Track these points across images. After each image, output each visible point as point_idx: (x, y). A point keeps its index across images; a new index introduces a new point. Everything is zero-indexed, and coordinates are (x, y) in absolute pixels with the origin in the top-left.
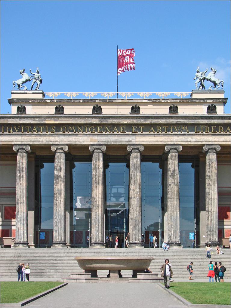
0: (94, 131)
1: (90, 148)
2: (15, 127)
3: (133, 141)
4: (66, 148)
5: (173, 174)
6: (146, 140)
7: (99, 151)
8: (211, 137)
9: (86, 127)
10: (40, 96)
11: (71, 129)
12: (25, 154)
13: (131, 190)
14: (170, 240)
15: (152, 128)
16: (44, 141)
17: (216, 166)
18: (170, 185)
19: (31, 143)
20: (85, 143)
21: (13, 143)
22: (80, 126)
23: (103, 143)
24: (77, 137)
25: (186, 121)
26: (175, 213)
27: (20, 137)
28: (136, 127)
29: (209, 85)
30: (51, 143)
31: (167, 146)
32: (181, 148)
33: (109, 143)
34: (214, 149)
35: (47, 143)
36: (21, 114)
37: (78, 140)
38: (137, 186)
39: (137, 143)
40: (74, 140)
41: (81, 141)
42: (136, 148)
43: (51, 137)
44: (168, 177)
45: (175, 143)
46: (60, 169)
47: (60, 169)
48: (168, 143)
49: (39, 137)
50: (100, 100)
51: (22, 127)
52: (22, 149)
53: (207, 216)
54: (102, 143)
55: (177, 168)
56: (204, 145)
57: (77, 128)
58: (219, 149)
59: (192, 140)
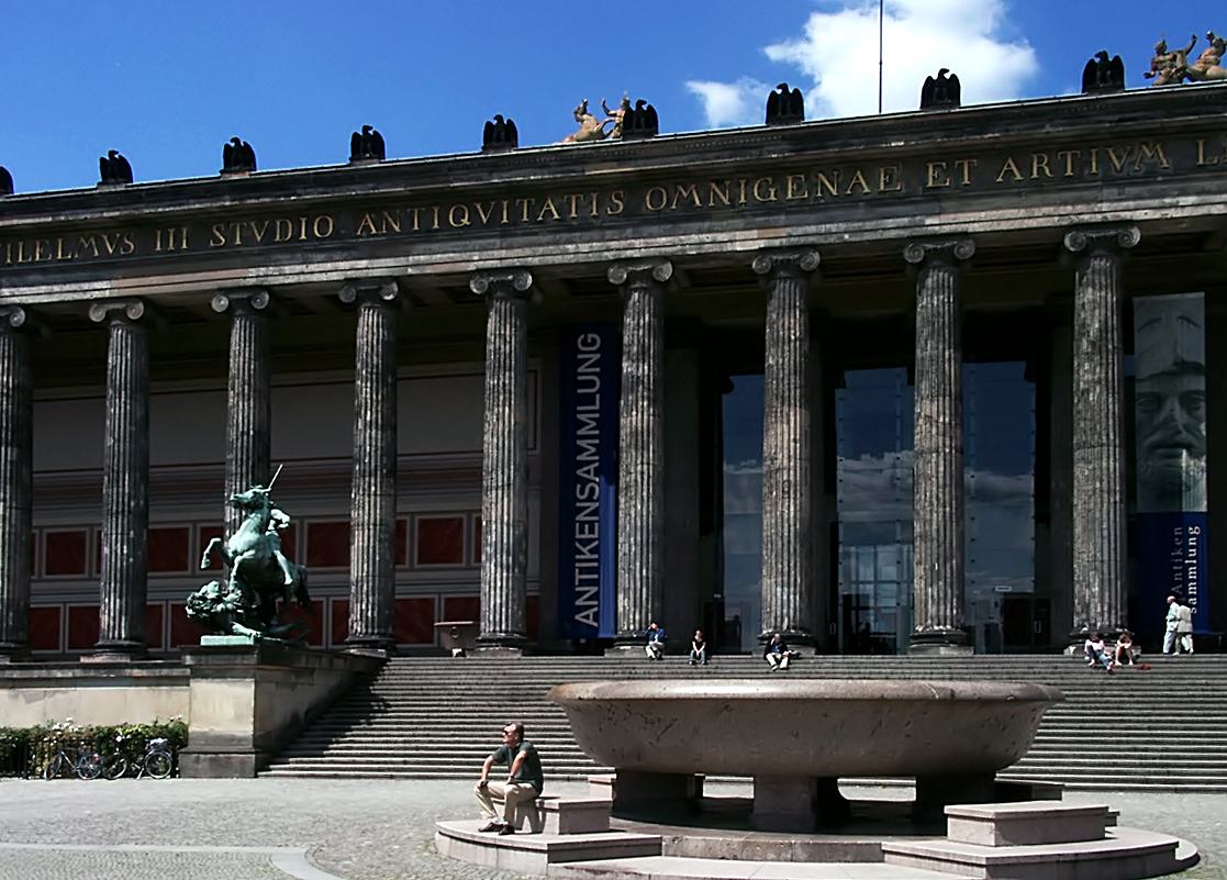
0: (772, 194)
2: (479, 207)
9: (743, 182)
11: (685, 194)
13: (921, 421)
14: (1088, 619)
15: (1010, 161)
18: (1087, 391)
22: (718, 182)
28: (944, 164)
44: (1076, 363)
47: (643, 351)
51: (505, 203)
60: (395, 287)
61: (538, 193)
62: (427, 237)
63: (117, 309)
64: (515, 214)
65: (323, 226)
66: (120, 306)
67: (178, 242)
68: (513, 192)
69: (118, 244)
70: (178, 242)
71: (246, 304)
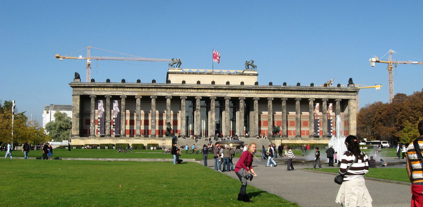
1: (210, 98)
5: (242, 109)
6: (231, 95)
7: (214, 99)
8: (256, 94)
10: (181, 71)
19: (187, 96)
20: (208, 96)
21: (180, 96)
23: (216, 96)
24: (205, 93)
25: (247, 88)
26: (243, 124)
27: (183, 93)
30: (195, 96)
34: (258, 99)
35: (193, 96)
37: (205, 95)
38: (228, 113)
40: (204, 95)
43: (195, 93)
45: (243, 96)
47: (199, 106)
48: (240, 96)
49: (191, 93)
50: (206, 73)
52: (184, 98)
53: (254, 125)
54: (215, 96)
56: (253, 98)
58: (259, 99)
60: (172, 97)
61: (187, 89)
62: (176, 92)
63: (138, 97)
66: (139, 96)
68: (185, 88)
71: (155, 97)
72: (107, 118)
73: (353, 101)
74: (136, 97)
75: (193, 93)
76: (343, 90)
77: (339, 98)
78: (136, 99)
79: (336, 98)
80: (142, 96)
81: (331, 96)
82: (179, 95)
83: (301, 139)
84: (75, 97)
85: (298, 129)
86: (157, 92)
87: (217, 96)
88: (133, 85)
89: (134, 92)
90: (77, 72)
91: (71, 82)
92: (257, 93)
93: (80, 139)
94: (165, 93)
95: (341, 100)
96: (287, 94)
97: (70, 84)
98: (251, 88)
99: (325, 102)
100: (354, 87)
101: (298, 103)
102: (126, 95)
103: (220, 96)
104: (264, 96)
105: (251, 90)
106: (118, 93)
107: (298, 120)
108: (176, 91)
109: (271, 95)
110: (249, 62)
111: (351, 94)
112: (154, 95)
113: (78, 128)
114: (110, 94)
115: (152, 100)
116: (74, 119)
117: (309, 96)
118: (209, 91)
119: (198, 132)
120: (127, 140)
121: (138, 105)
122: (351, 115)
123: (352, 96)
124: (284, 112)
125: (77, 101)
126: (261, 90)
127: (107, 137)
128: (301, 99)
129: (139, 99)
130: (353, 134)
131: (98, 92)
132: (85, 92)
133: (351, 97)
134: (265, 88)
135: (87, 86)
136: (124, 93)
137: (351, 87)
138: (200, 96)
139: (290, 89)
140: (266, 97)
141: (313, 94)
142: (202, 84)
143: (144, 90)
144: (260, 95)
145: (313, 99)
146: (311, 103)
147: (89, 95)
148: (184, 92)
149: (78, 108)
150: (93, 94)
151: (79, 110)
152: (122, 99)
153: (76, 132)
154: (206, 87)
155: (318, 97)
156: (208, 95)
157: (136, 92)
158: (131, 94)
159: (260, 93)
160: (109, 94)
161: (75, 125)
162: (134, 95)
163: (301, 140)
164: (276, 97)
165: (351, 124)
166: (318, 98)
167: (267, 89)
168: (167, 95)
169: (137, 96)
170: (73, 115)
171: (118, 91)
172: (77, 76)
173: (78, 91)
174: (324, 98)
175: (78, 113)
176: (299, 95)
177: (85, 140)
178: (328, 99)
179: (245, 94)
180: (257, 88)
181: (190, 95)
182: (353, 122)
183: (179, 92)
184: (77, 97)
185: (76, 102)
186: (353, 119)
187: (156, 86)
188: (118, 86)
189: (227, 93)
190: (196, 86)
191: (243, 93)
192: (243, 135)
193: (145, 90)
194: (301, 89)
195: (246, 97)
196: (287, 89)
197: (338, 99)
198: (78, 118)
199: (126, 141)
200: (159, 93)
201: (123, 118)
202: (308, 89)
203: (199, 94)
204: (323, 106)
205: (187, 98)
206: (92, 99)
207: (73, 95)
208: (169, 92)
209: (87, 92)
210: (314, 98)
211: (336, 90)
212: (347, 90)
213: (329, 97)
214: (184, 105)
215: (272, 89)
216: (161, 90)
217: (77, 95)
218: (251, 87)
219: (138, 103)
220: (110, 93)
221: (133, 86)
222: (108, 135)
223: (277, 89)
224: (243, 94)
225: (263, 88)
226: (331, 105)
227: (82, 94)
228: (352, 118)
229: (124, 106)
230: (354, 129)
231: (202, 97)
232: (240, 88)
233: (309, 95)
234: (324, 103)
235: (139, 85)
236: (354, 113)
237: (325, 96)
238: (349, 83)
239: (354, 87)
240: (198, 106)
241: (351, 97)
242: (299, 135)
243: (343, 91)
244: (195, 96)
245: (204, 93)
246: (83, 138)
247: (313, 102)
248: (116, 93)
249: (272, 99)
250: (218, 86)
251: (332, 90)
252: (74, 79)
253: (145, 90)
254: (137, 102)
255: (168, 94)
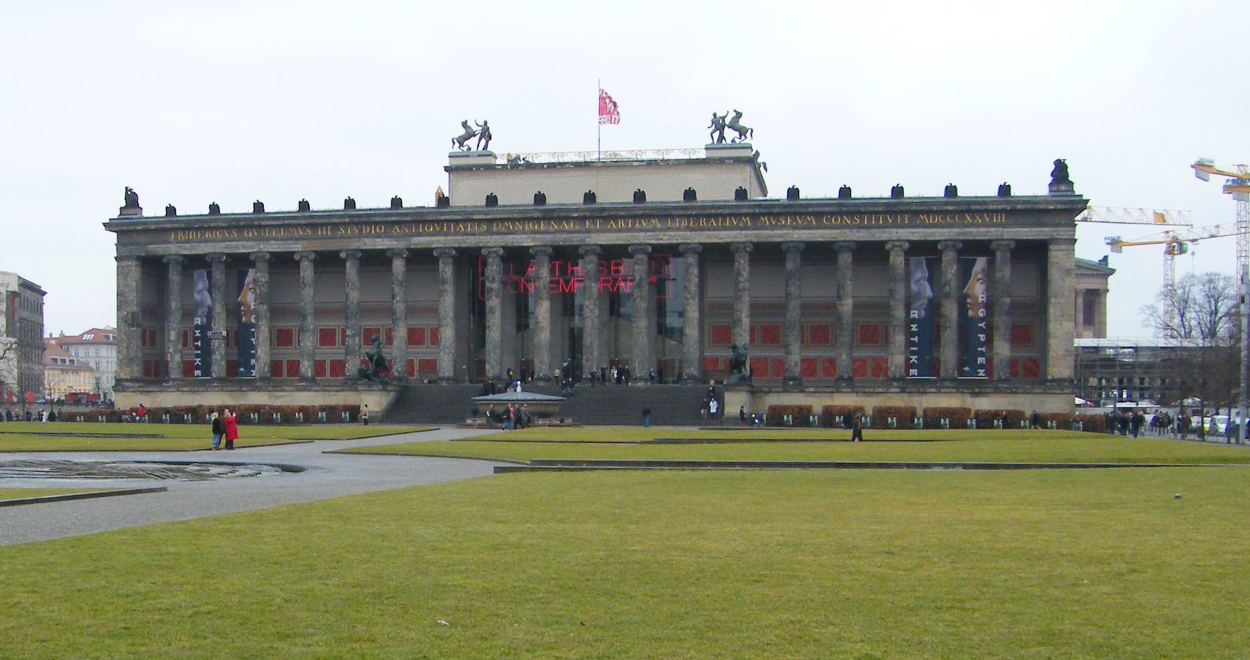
1: (530, 251)
3: (587, 240)
4: (501, 252)
8: (689, 233)
12: (450, 260)
16: (473, 242)
17: (696, 272)
20: (525, 244)
21: (433, 246)
23: (550, 243)
24: (514, 236)
25: (654, 212)
27: (443, 238)
29: (730, 134)
30: (481, 245)
31: (633, 247)
32: (650, 249)
33: (556, 244)
35: (476, 246)
36: (443, 208)
37: (515, 240)
39: (593, 243)
40: (511, 241)
41: (520, 241)
42: (590, 249)
43: (482, 237)
45: (643, 241)
46: (493, 281)
48: (632, 242)
55: (644, 276)
56: (678, 245)
57: (515, 224)
59: (664, 238)
60: (407, 253)
61: (457, 222)
62: (419, 235)
63: (304, 255)
64: (449, 228)
65: (380, 228)
66: (305, 254)
67: (327, 231)
69: (304, 231)
70: (327, 231)
71: (353, 255)
72: (215, 325)
73: (1063, 247)
74: (297, 257)
75: (474, 237)
76: (1019, 207)
77: (1005, 237)
78: (297, 264)
79: (995, 237)
80: (316, 252)
81: (974, 230)
82: (430, 246)
83: (849, 390)
84: (123, 263)
85: (841, 355)
86: (360, 236)
87: (555, 242)
88: (284, 218)
89: (292, 242)
90: (130, 187)
91: (110, 220)
92: (693, 230)
93: (138, 393)
94: (385, 240)
95: (1013, 245)
96: (805, 228)
97: (104, 224)
98: (669, 212)
99: (951, 253)
100: (1069, 193)
101: (845, 259)
102: (271, 253)
103: (565, 241)
104: (718, 238)
105: (672, 217)
106: (244, 247)
107: (844, 321)
108: (421, 230)
109: (743, 232)
110: (723, 118)
111: (1057, 220)
112: (352, 248)
113: (133, 359)
114: (220, 251)
115: (348, 265)
116: (123, 331)
117: (885, 232)
118: (529, 226)
119: (492, 368)
120: (272, 393)
121: (303, 282)
122: (1053, 300)
123: (1060, 229)
124: (790, 294)
125: (130, 275)
126: (708, 216)
127: (215, 384)
128: (854, 246)
129: (306, 263)
130: (1061, 372)
131: (188, 245)
132: (152, 246)
133: (1055, 233)
134: (719, 211)
135: (153, 227)
136: (261, 246)
137: (1056, 194)
138: (496, 244)
139: (810, 210)
140: (728, 240)
141: (902, 226)
142: (504, 206)
143: (320, 233)
144: (704, 236)
145: (902, 243)
146: (897, 260)
147: (162, 257)
148: (446, 234)
149: (132, 298)
150: (173, 252)
151: (135, 302)
152: (258, 264)
153: (128, 370)
154: (516, 216)
155: (921, 235)
156: (523, 242)
157: (299, 242)
158: (281, 246)
159: (702, 229)
160: (218, 250)
161: (125, 350)
162: (293, 250)
163: (853, 392)
164: (762, 240)
165: (1053, 335)
166: (923, 239)
167: (727, 211)
168: (392, 247)
169: (302, 252)
170: (118, 318)
171: (243, 240)
172: (132, 199)
173: (132, 244)
174: (947, 240)
175: (133, 314)
176: (847, 231)
177: (151, 394)
178: (961, 241)
179: (648, 234)
180: (689, 213)
181: (467, 242)
182: (1061, 325)
183: (430, 235)
184: (130, 263)
185: (126, 277)
186: (1063, 315)
187: (356, 220)
188: (242, 223)
189: (588, 231)
190: (480, 214)
191: (641, 230)
192: (643, 374)
193: (324, 233)
194: (853, 209)
195: (653, 246)
196: (798, 210)
197: (1000, 242)
198: (133, 326)
199: (270, 398)
200: (366, 240)
201: (260, 323)
202: (881, 209)
203: (494, 241)
204: (943, 265)
205: (454, 252)
206: (170, 266)
207: (116, 258)
208: (398, 237)
209: (158, 249)
210: (905, 238)
211: (991, 207)
212: (1037, 207)
213: (965, 234)
214: (446, 276)
215: (745, 211)
216: (373, 232)
217: (128, 258)
218: (666, 209)
219: (304, 277)
220: (221, 248)
221: (286, 222)
222: (219, 380)
223: (763, 211)
224: (642, 234)
225: (713, 211)
226: (980, 263)
227: (143, 254)
228: (1059, 314)
229: (263, 286)
230: (1064, 352)
231: (503, 247)
232: (632, 213)
233: (887, 230)
234: (949, 258)
235: (305, 218)
236: (1067, 293)
237: (950, 232)
238: (1052, 178)
239: (1069, 193)
240: (491, 278)
241: (1055, 233)
242: (846, 376)
243: (1021, 211)
244: (482, 248)
245: (511, 236)
246: (146, 389)
247: (903, 253)
248: (237, 247)
249: (745, 248)
250: (554, 210)
251: (973, 207)
252: (121, 208)
253: (324, 233)
254: (302, 274)
255: (395, 243)
